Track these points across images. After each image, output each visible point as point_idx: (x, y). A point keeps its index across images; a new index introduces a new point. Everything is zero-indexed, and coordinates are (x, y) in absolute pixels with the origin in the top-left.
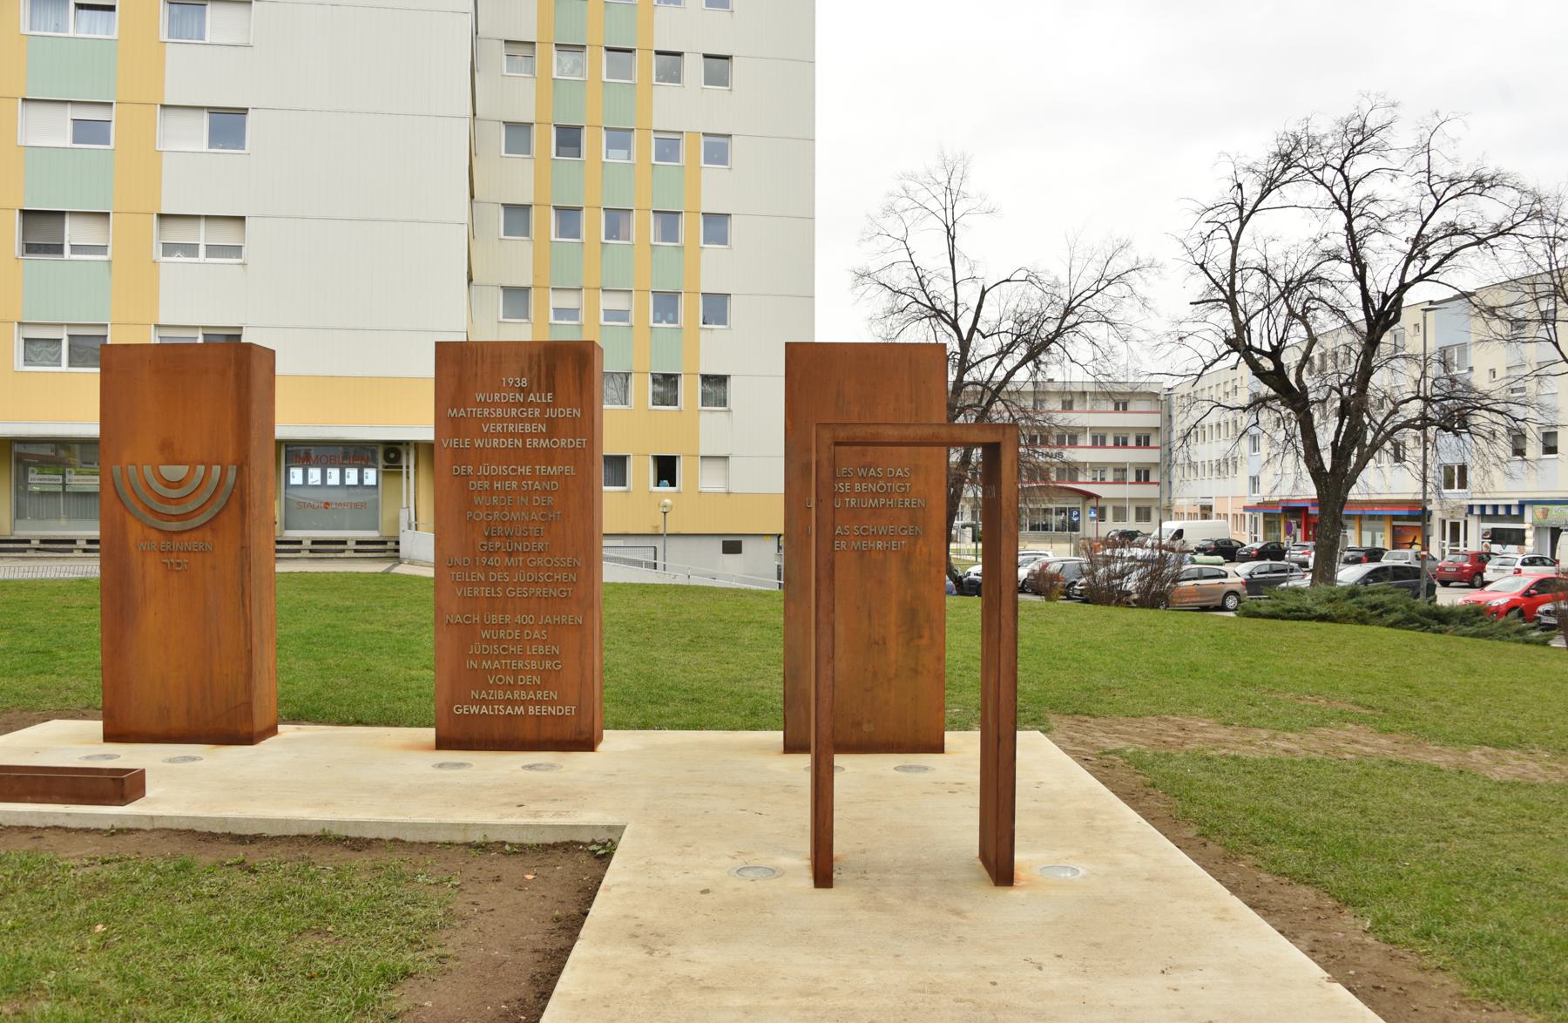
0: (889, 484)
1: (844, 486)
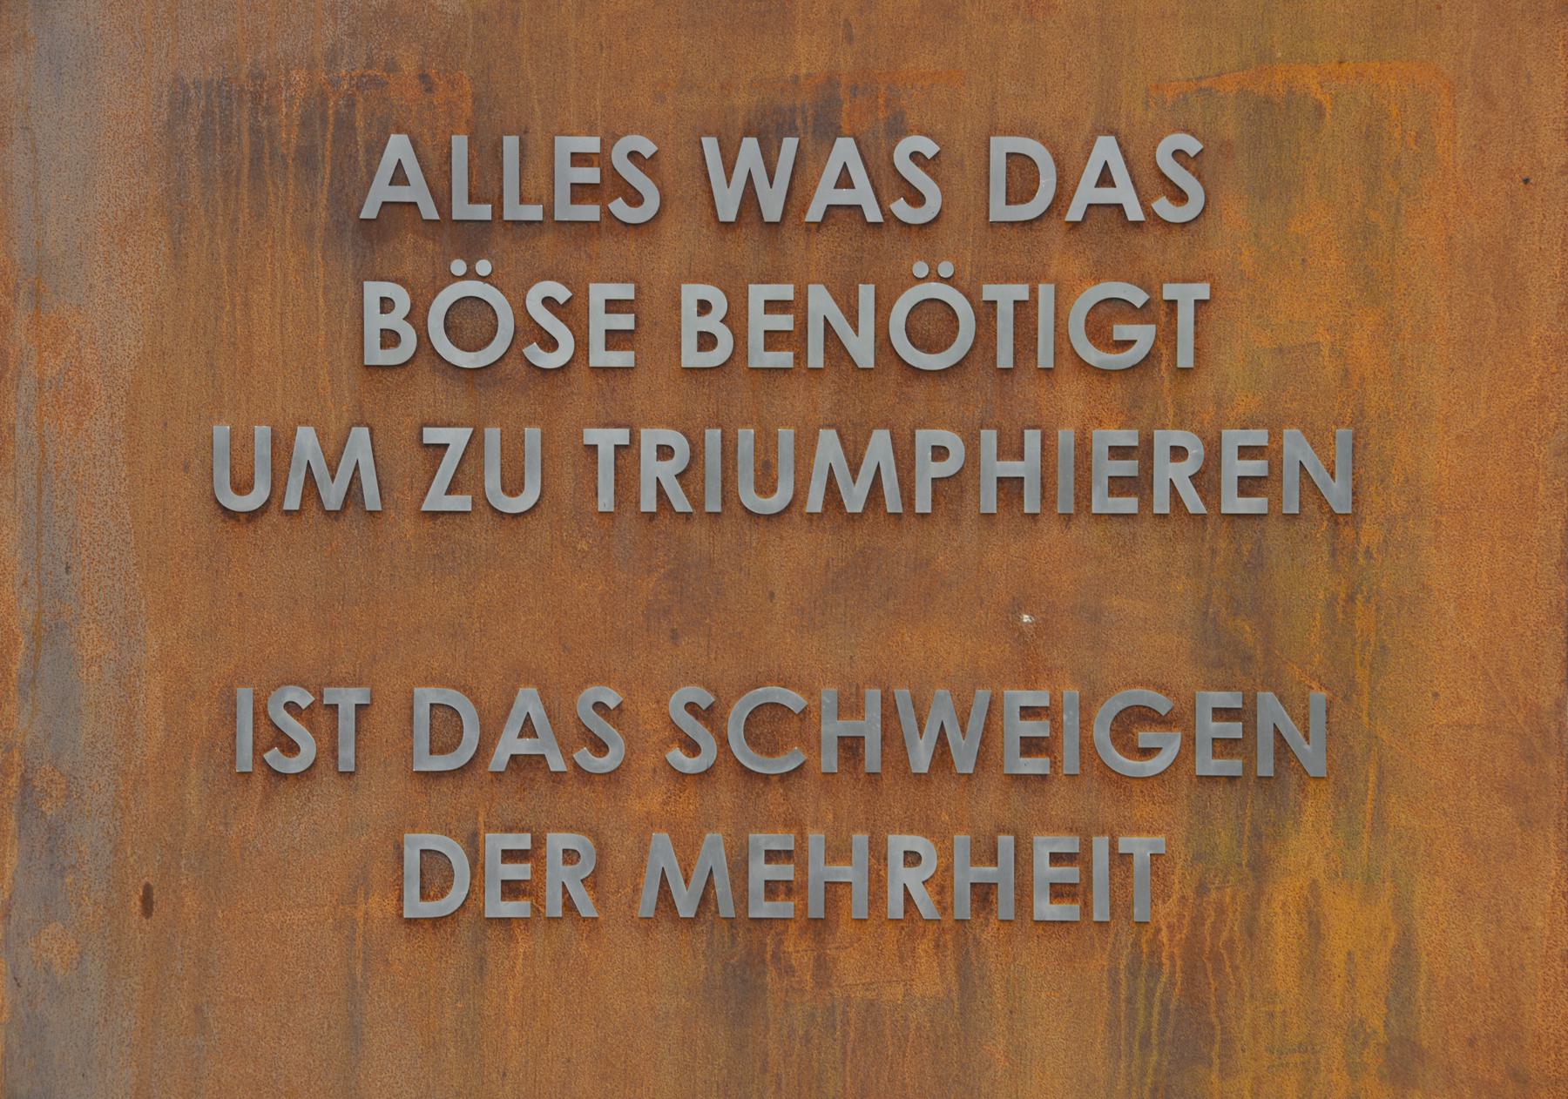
0: (1003, 295)
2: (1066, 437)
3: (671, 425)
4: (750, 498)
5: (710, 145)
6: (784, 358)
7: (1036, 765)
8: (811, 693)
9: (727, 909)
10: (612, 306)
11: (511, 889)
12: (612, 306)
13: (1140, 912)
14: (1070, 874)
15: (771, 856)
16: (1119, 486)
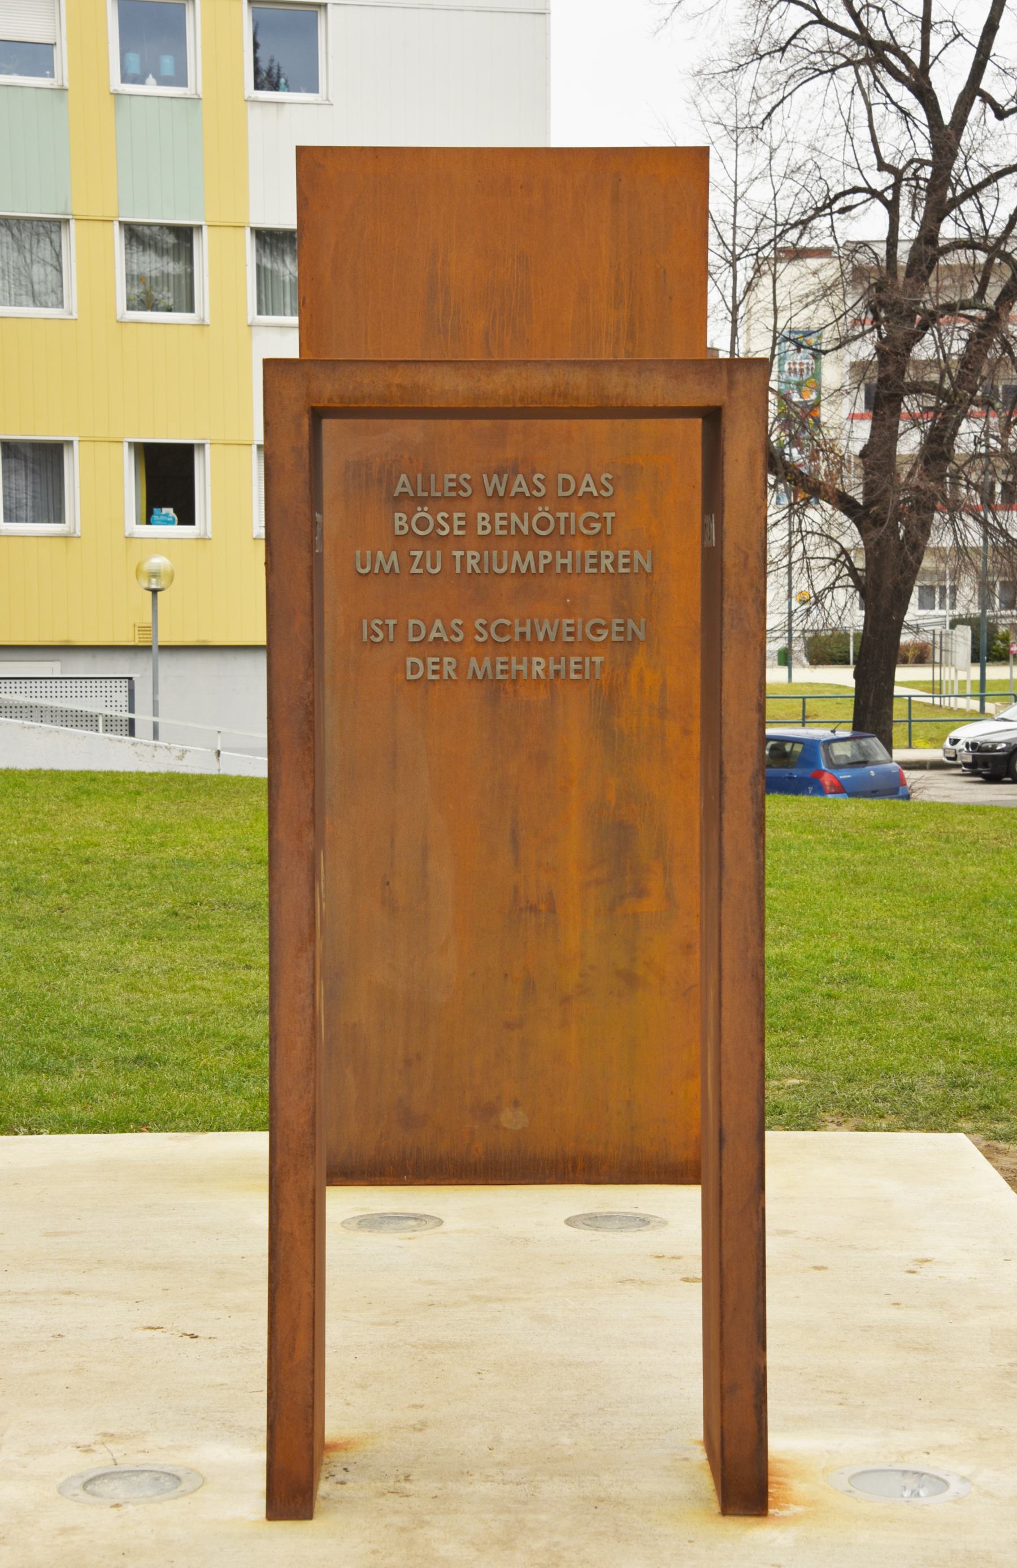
0: (562, 515)
1: (449, 520)
2: (578, 553)
3: (476, 550)
4: (496, 570)
5: (485, 476)
6: (504, 532)
7: (571, 639)
8: (512, 621)
9: (491, 677)
10: (460, 519)
11: (434, 672)
12: (460, 519)
13: (597, 676)
14: (579, 667)
15: (502, 663)
16: (592, 566)
